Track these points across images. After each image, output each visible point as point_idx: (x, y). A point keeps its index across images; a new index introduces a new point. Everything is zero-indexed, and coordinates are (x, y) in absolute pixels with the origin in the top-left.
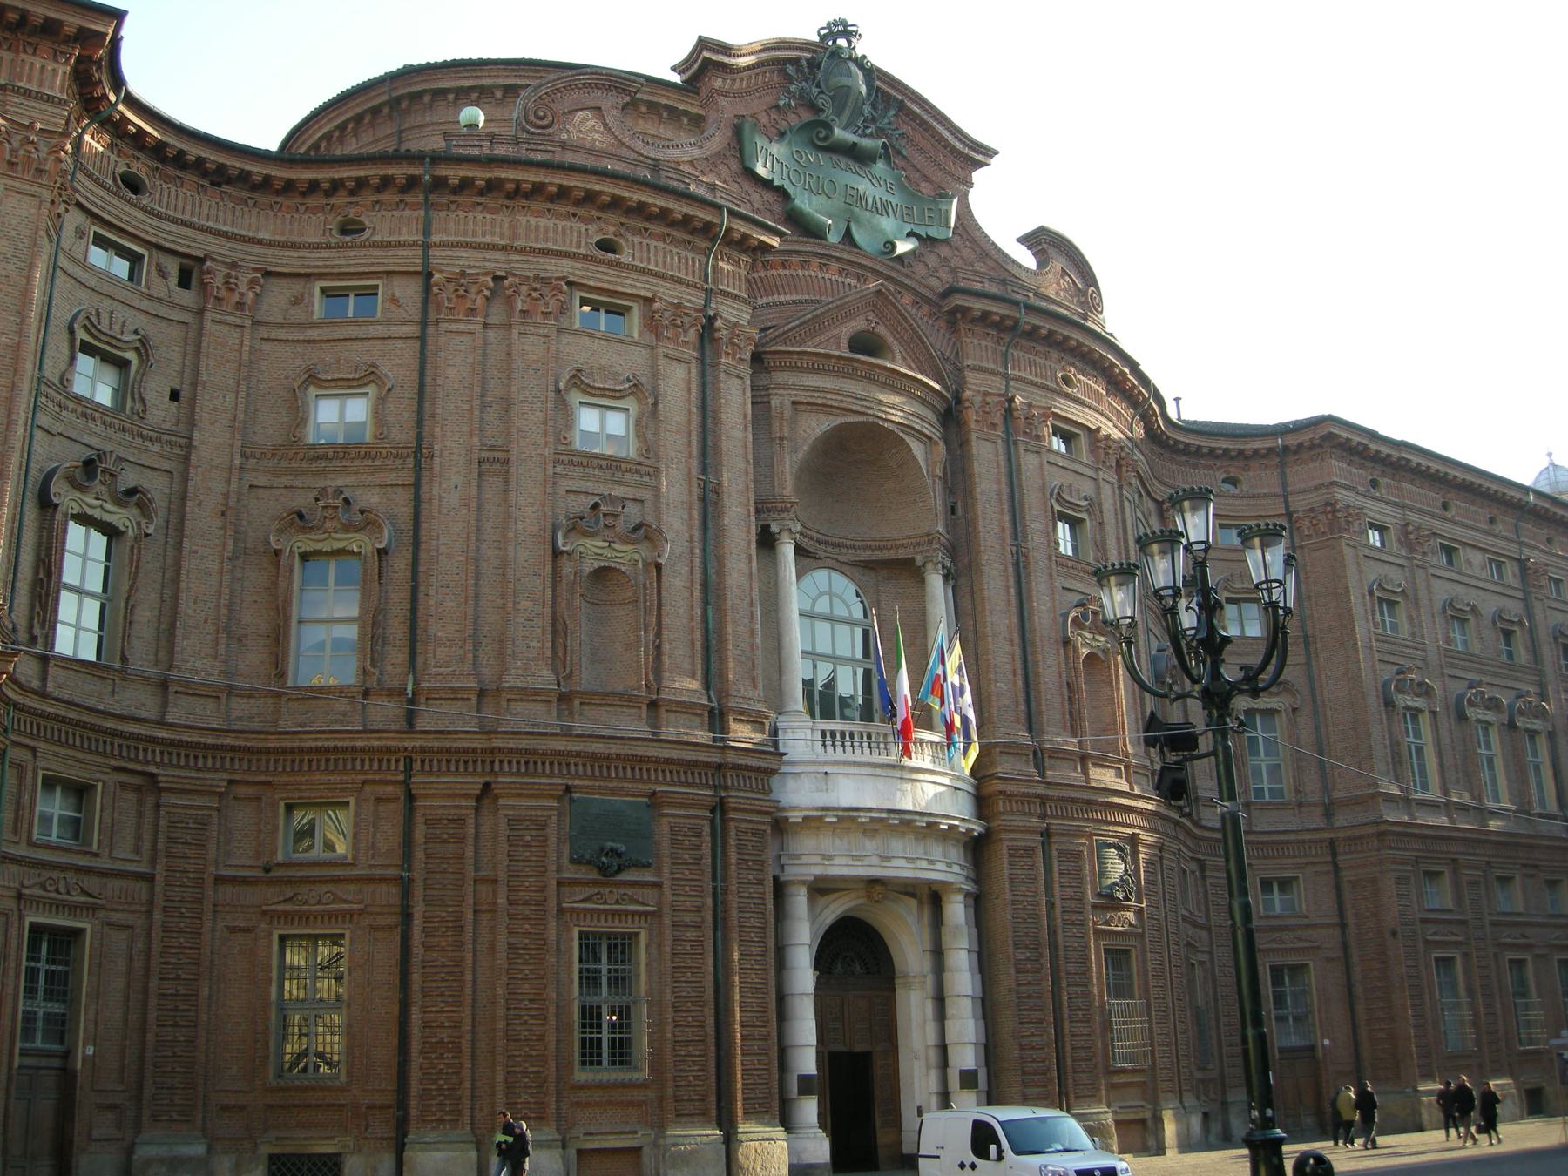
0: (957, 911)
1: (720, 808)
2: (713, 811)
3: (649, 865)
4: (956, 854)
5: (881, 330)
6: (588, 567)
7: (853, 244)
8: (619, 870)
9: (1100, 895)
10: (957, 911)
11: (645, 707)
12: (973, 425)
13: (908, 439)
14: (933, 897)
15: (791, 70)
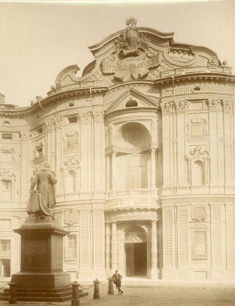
0: (154, 225)
1: (92, 211)
2: (90, 212)
3: (77, 223)
4: (155, 213)
5: (134, 99)
6: (68, 170)
7: (134, 78)
8: (73, 224)
9: (193, 219)
10: (154, 225)
11: (77, 195)
12: (163, 112)
13: (142, 123)
14: (148, 223)
15: (116, 41)
